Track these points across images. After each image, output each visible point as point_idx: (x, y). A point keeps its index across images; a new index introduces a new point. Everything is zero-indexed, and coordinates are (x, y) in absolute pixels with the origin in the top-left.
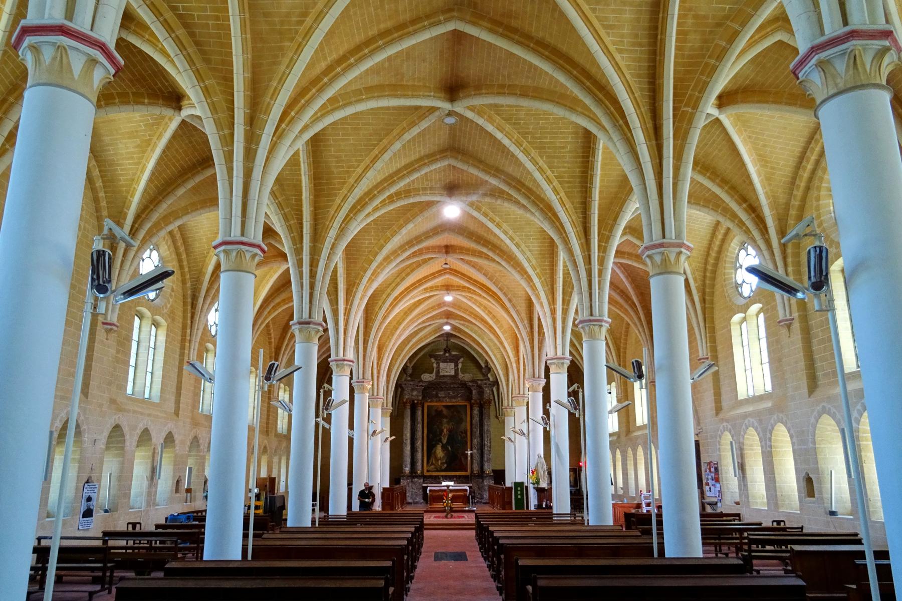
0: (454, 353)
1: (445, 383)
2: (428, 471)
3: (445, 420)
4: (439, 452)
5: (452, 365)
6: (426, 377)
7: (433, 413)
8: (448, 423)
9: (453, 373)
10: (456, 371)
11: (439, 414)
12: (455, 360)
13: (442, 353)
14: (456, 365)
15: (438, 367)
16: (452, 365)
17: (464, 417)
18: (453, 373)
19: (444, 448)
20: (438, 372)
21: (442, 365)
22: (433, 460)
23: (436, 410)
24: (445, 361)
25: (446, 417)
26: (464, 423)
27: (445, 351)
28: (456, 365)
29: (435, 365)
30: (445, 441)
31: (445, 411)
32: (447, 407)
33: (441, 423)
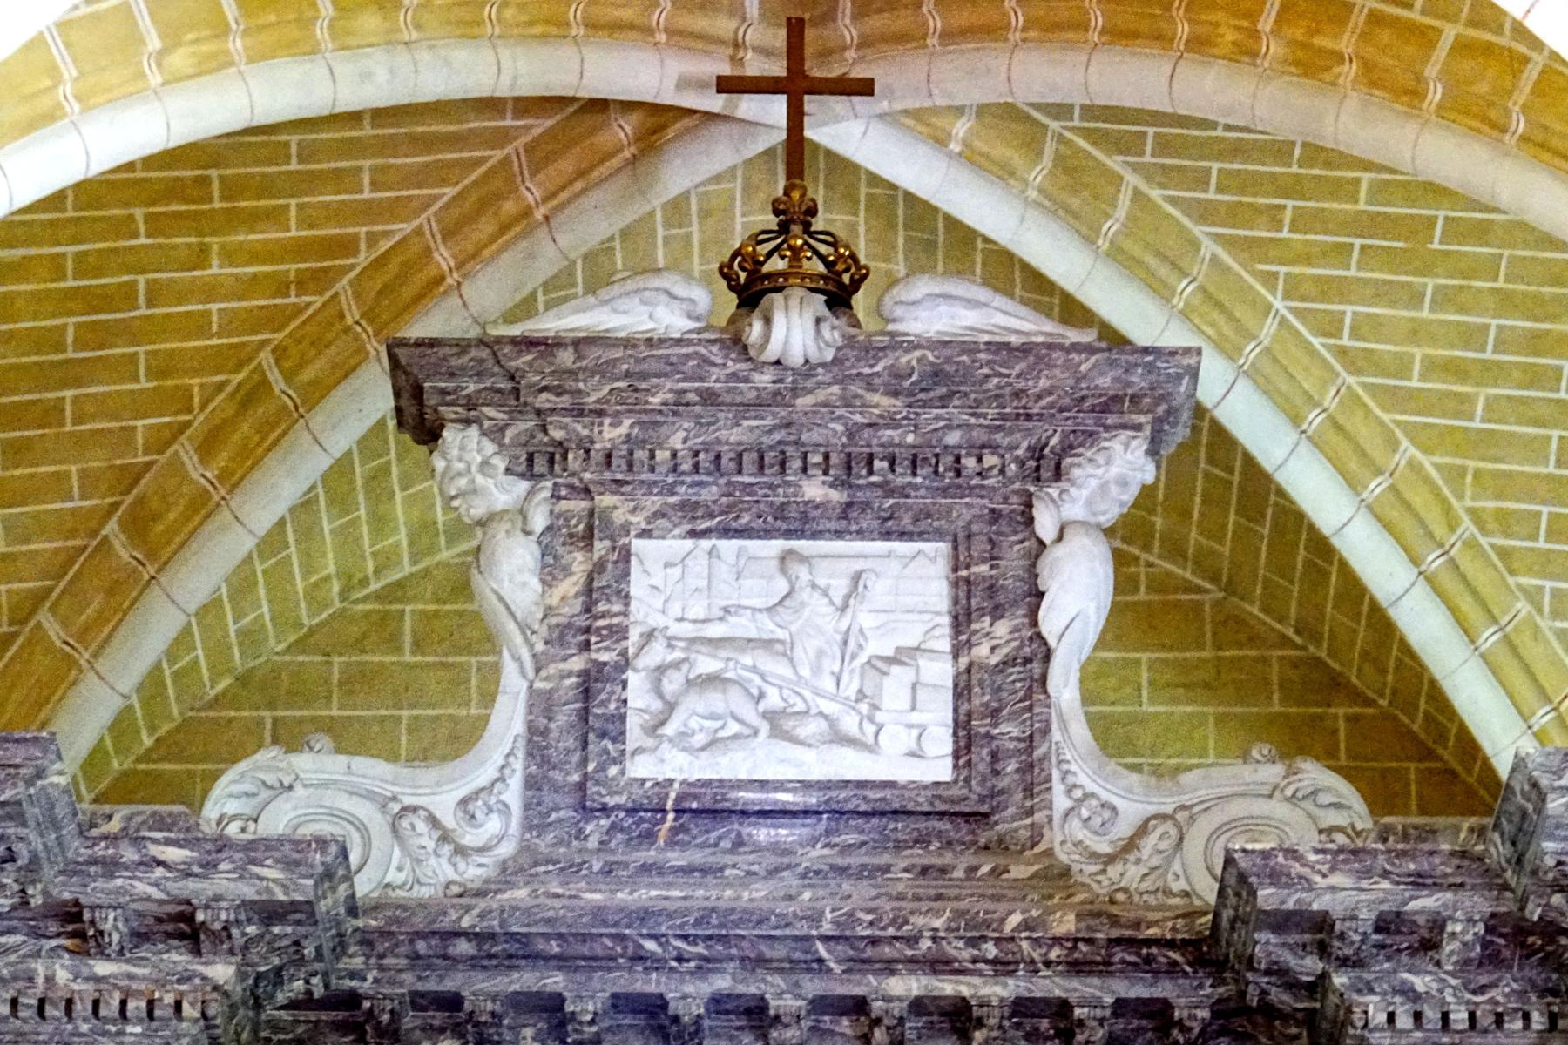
0: (937, 312)
1: (717, 938)
5: (906, 586)
6: (291, 796)
9: (913, 748)
10: (996, 708)
12: (951, 462)
13: (668, 308)
14: (1000, 584)
15: (592, 626)
16: (906, 586)
18: (913, 748)
20: (588, 709)
21: (678, 583)
24: (748, 498)
27: (751, 288)
28: (1000, 584)
29: (515, 578)
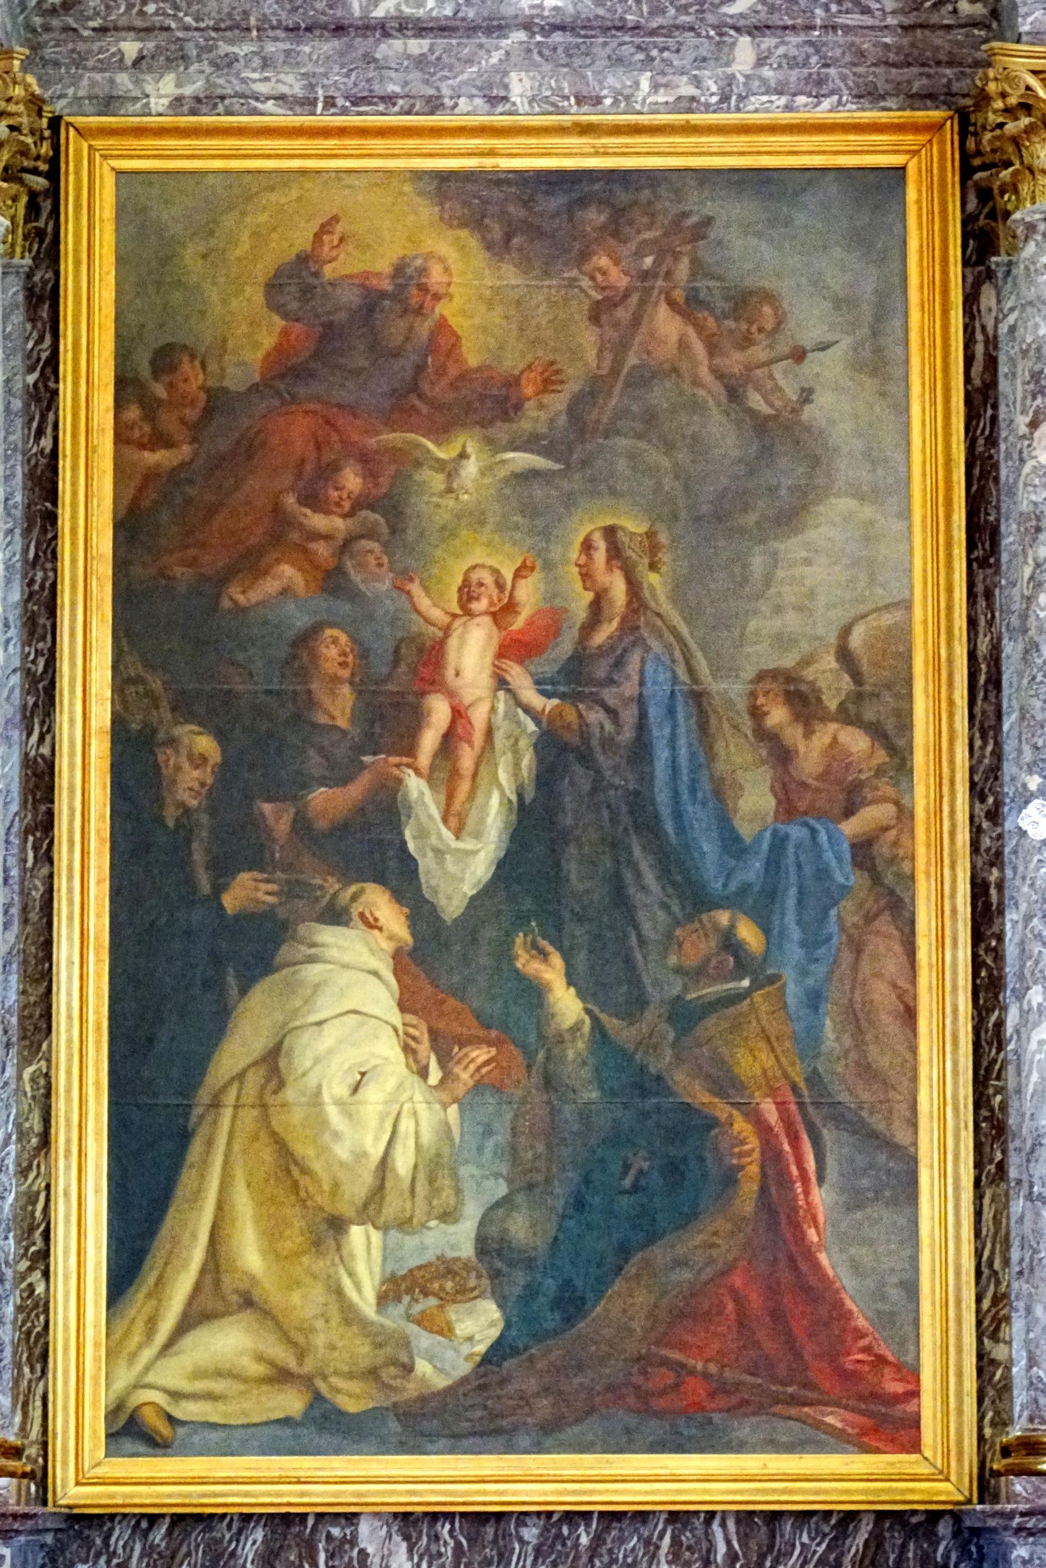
2: (129, 1430)
3: (467, 469)
4: (352, 1052)
7: (246, 335)
8: (532, 509)
11: (354, 343)
17: (836, 405)
19: (449, 978)
22: (221, 1198)
23: (296, 282)
25: (491, 404)
26: (834, 521)
30: (463, 855)
31: (475, 298)
32: (537, 216)
33: (389, 509)
